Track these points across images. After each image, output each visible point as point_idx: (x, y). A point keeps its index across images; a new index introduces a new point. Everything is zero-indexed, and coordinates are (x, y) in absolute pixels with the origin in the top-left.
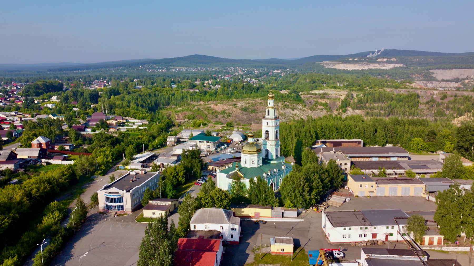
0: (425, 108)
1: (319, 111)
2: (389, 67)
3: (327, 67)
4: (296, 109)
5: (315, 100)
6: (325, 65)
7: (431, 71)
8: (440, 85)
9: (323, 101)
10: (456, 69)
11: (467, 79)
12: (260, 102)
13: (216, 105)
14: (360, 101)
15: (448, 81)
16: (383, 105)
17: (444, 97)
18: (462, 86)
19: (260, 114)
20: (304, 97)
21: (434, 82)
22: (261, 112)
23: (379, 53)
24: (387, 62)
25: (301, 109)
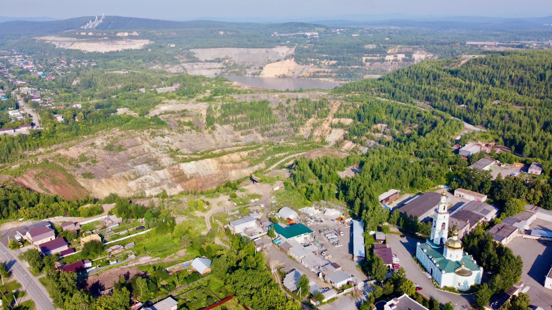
0: (277, 113)
1: (189, 133)
2: (138, 45)
3: (61, 46)
4: (165, 135)
5: (177, 119)
6: (57, 44)
7: (192, 50)
8: (205, 66)
9: (187, 120)
10: (213, 47)
11: (227, 59)
12: (120, 133)
13: (67, 149)
14: (224, 115)
15: (211, 61)
16: (243, 116)
17: (288, 101)
18: (225, 67)
19: (130, 150)
20: (163, 118)
21: (199, 63)
22: (129, 147)
23: (101, 21)
24: (131, 37)
25: (169, 134)
